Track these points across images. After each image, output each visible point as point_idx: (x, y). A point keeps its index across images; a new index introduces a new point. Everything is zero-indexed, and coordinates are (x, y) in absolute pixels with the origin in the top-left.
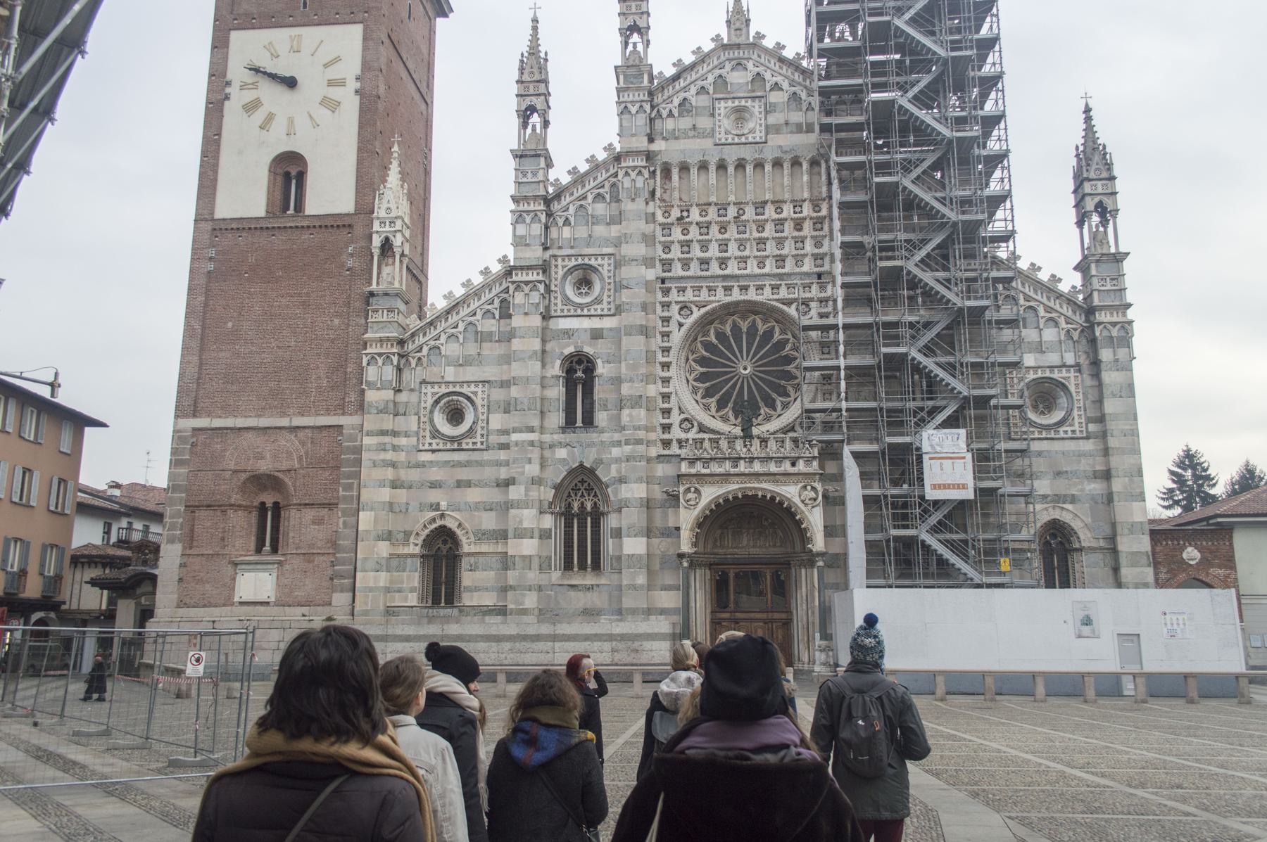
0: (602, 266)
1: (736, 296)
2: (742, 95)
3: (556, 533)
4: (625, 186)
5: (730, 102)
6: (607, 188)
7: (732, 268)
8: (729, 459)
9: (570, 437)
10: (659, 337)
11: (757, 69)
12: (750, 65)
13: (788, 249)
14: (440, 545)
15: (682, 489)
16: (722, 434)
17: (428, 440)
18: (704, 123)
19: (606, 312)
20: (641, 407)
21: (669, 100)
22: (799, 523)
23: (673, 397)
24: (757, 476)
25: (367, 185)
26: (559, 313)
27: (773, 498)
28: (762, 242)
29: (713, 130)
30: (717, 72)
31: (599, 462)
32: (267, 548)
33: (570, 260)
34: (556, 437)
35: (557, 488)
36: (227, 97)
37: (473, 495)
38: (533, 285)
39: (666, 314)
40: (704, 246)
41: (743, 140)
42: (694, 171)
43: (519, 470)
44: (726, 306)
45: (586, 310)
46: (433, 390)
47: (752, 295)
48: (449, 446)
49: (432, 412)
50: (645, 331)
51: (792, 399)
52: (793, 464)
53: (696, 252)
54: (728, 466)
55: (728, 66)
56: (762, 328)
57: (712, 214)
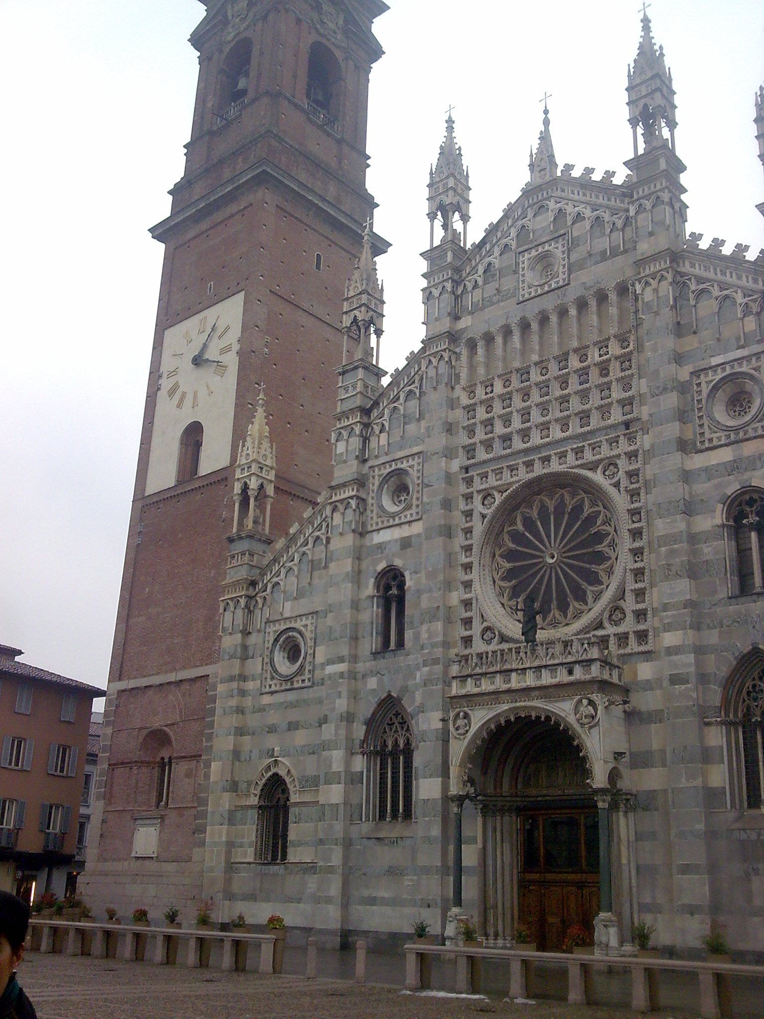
0: (411, 467)
1: (539, 470)
2: (544, 240)
3: (368, 777)
4: (429, 375)
5: (533, 250)
6: (417, 384)
7: (536, 439)
8: (500, 672)
9: (382, 663)
10: (461, 535)
11: (559, 205)
12: (552, 204)
13: (595, 400)
14: (280, 795)
15: (452, 714)
17: (269, 682)
18: (508, 283)
19: (415, 517)
20: (438, 620)
21: (474, 269)
22: (578, 748)
23: (474, 602)
24: (527, 691)
25: (239, 435)
26: (374, 527)
27: (548, 718)
28: (564, 400)
29: (517, 288)
30: (520, 223)
31: (405, 689)
32: (163, 803)
33: (385, 468)
34: (368, 664)
35: (369, 723)
36: (159, 389)
37: (301, 738)
38: (345, 502)
39: (468, 508)
40: (507, 422)
41: (546, 288)
42: (499, 340)
43: (332, 706)
44: (529, 484)
45: (397, 519)
46: (275, 629)
47: (555, 466)
48: (283, 688)
49: (272, 652)
50: (448, 532)
51: (604, 586)
52: (570, 672)
53: (499, 429)
54: (499, 684)
55: (530, 214)
56: (570, 503)
57: (516, 383)
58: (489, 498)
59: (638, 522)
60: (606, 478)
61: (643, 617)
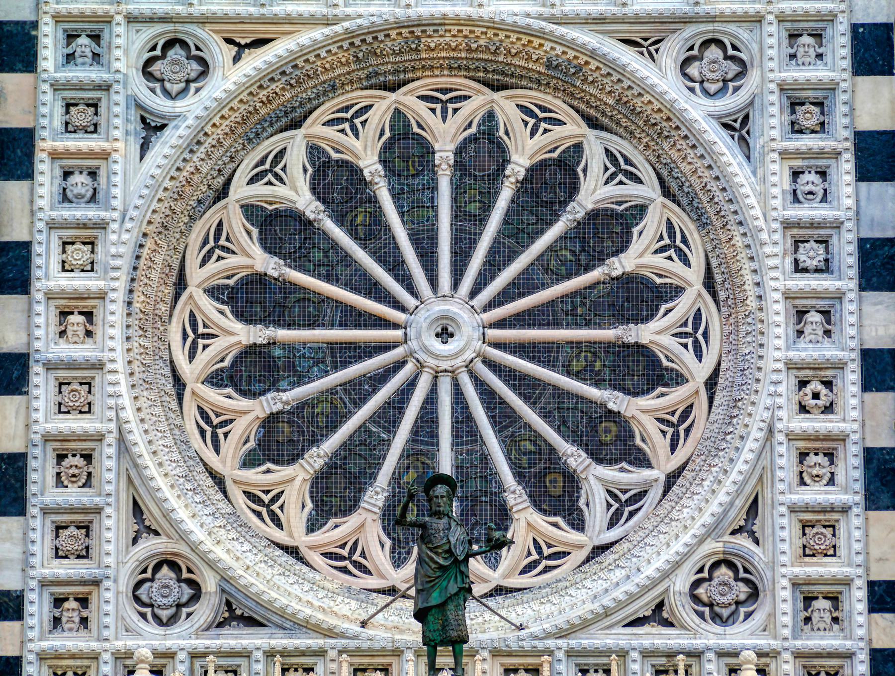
16: (330, 633)
23: (107, 453)
51: (656, 474)
58: (176, 53)
59: (817, 270)
60: (692, 90)
61: (827, 604)
